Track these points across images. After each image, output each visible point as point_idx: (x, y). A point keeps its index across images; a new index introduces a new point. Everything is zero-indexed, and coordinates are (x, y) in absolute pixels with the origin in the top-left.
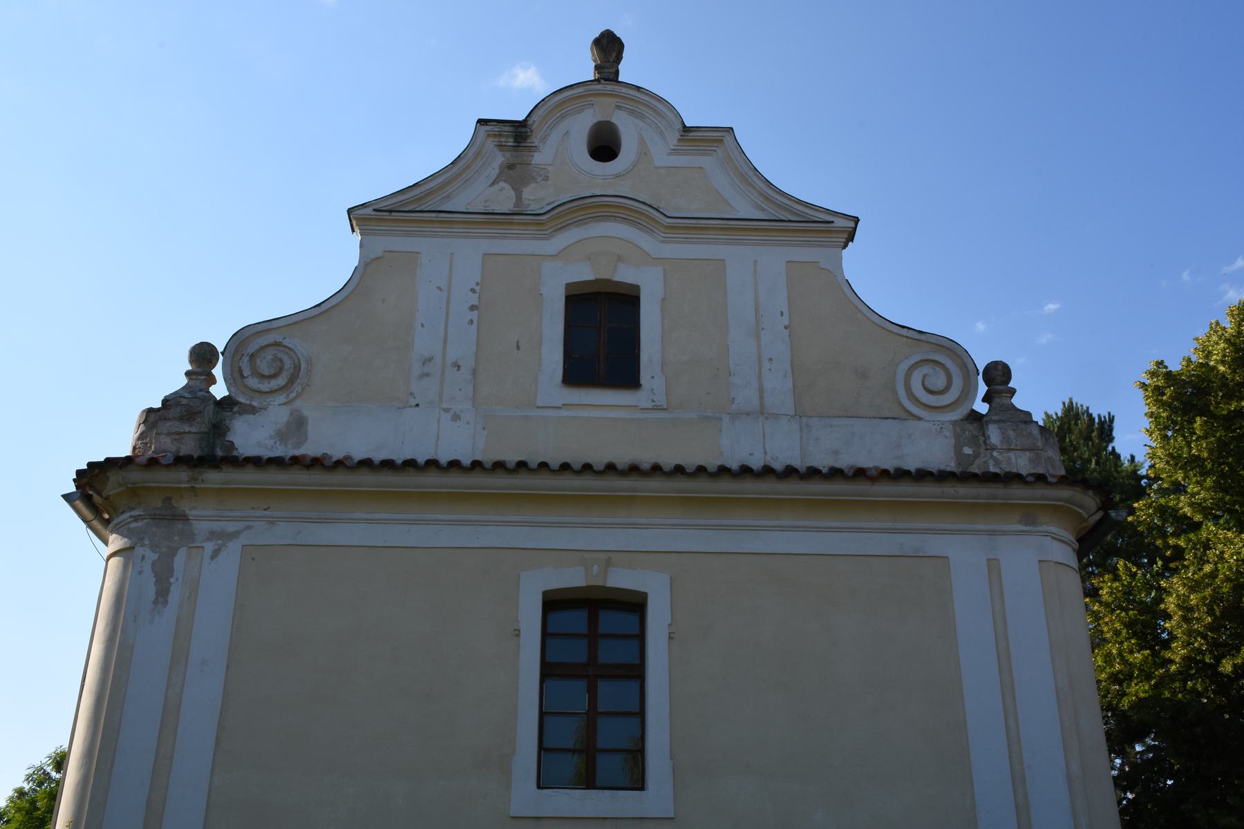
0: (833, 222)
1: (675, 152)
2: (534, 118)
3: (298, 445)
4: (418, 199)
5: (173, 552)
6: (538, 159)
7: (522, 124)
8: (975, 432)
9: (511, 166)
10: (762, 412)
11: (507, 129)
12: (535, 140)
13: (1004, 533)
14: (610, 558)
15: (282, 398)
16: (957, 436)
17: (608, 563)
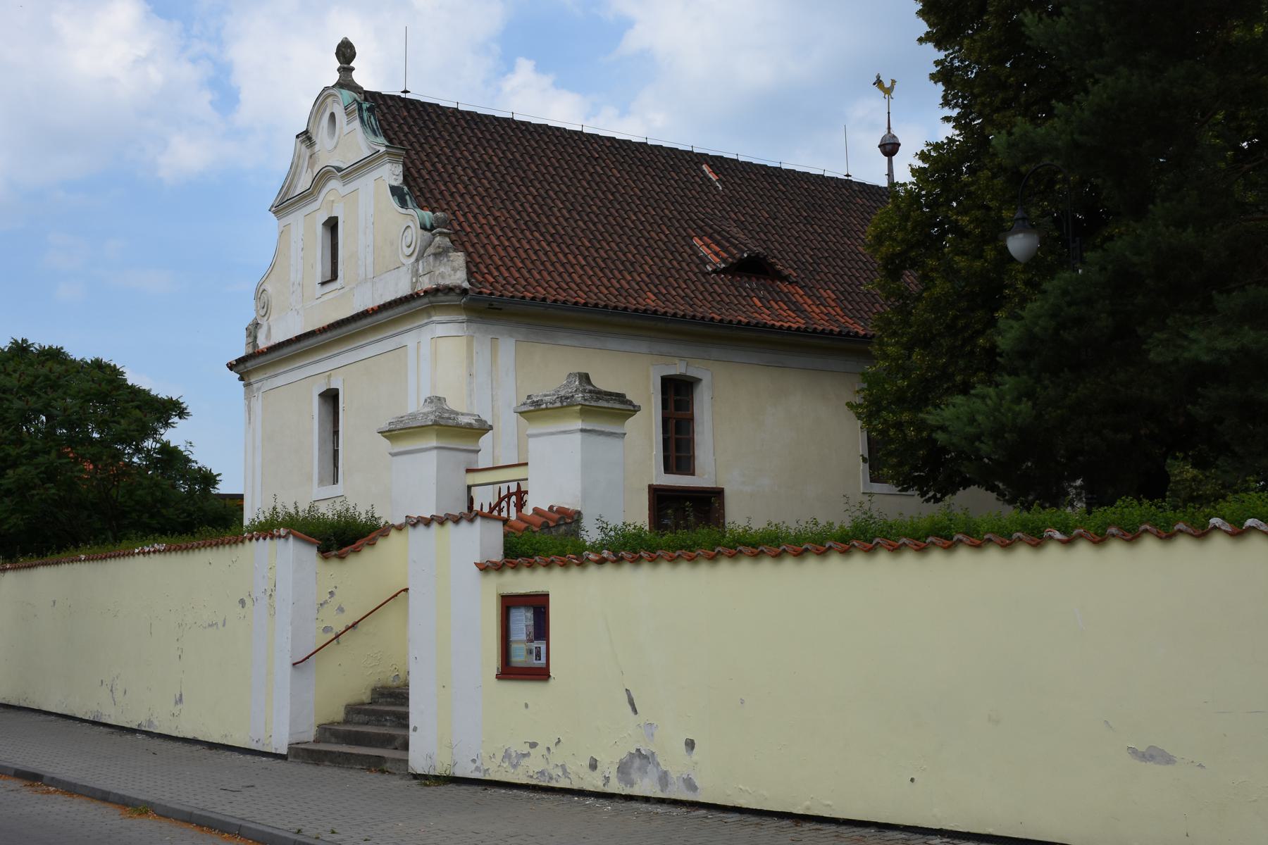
0: (379, 151)
1: (348, 123)
2: (310, 125)
3: (270, 339)
4: (283, 198)
5: (250, 401)
6: (317, 148)
7: (306, 132)
9: (311, 156)
10: (366, 280)
11: (304, 137)
12: (314, 138)
13: (422, 326)
14: (330, 374)
15: (266, 318)
16: (412, 272)
17: (329, 376)
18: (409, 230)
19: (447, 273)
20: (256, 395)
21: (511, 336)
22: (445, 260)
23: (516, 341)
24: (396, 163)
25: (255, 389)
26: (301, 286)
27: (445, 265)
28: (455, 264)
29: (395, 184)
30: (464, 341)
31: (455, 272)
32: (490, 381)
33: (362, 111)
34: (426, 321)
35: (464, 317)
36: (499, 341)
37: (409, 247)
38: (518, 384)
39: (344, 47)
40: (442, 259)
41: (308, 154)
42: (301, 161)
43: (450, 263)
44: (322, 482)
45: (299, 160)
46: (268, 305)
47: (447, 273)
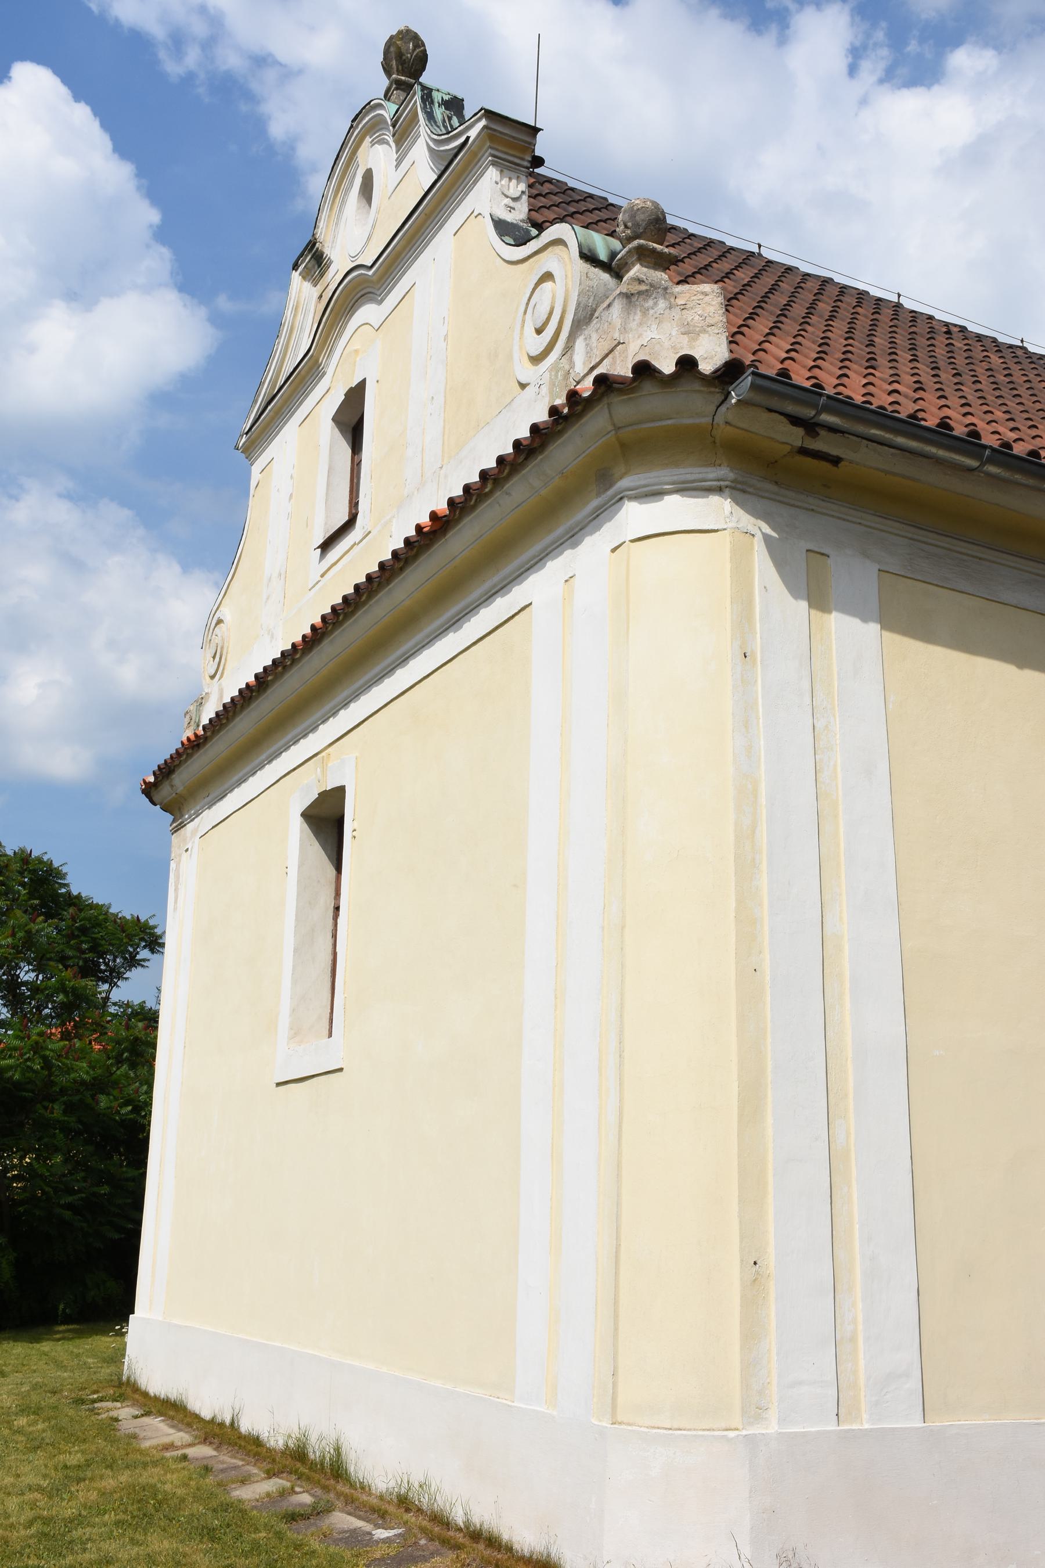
8: (567, 367)
15: (218, 676)
18: (548, 285)
19: (667, 344)
20: (189, 846)
21: (865, 555)
22: (662, 304)
23: (879, 570)
24: (509, 169)
25: (188, 835)
26: (283, 577)
27: (659, 320)
28: (692, 316)
29: (509, 217)
30: (721, 545)
31: (695, 340)
32: (806, 685)
33: (432, 102)
34: (595, 503)
35: (724, 472)
36: (829, 561)
37: (539, 331)
38: (890, 706)
39: (402, 39)
40: (650, 303)
41: (316, 295)
42: (299, 317)
43: (676, 313)
44: (297, 1033)
45: (295, 315)
46: (222, 648)
47: (667, 344)
